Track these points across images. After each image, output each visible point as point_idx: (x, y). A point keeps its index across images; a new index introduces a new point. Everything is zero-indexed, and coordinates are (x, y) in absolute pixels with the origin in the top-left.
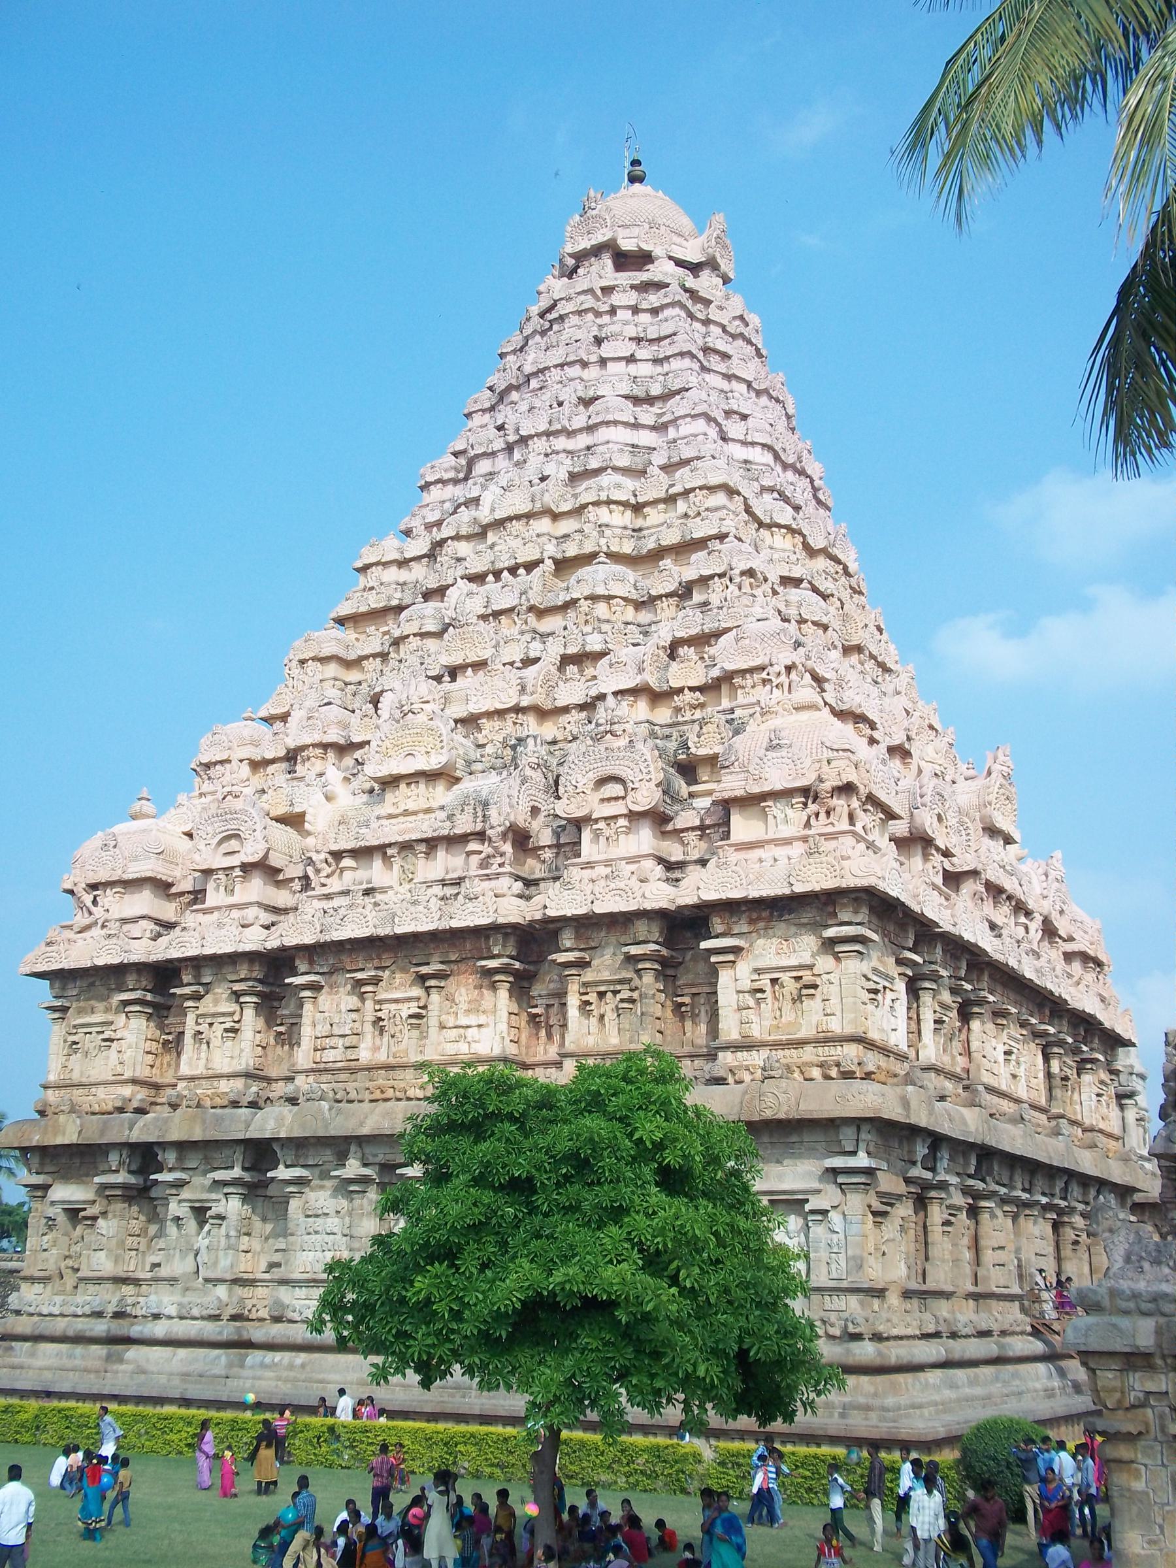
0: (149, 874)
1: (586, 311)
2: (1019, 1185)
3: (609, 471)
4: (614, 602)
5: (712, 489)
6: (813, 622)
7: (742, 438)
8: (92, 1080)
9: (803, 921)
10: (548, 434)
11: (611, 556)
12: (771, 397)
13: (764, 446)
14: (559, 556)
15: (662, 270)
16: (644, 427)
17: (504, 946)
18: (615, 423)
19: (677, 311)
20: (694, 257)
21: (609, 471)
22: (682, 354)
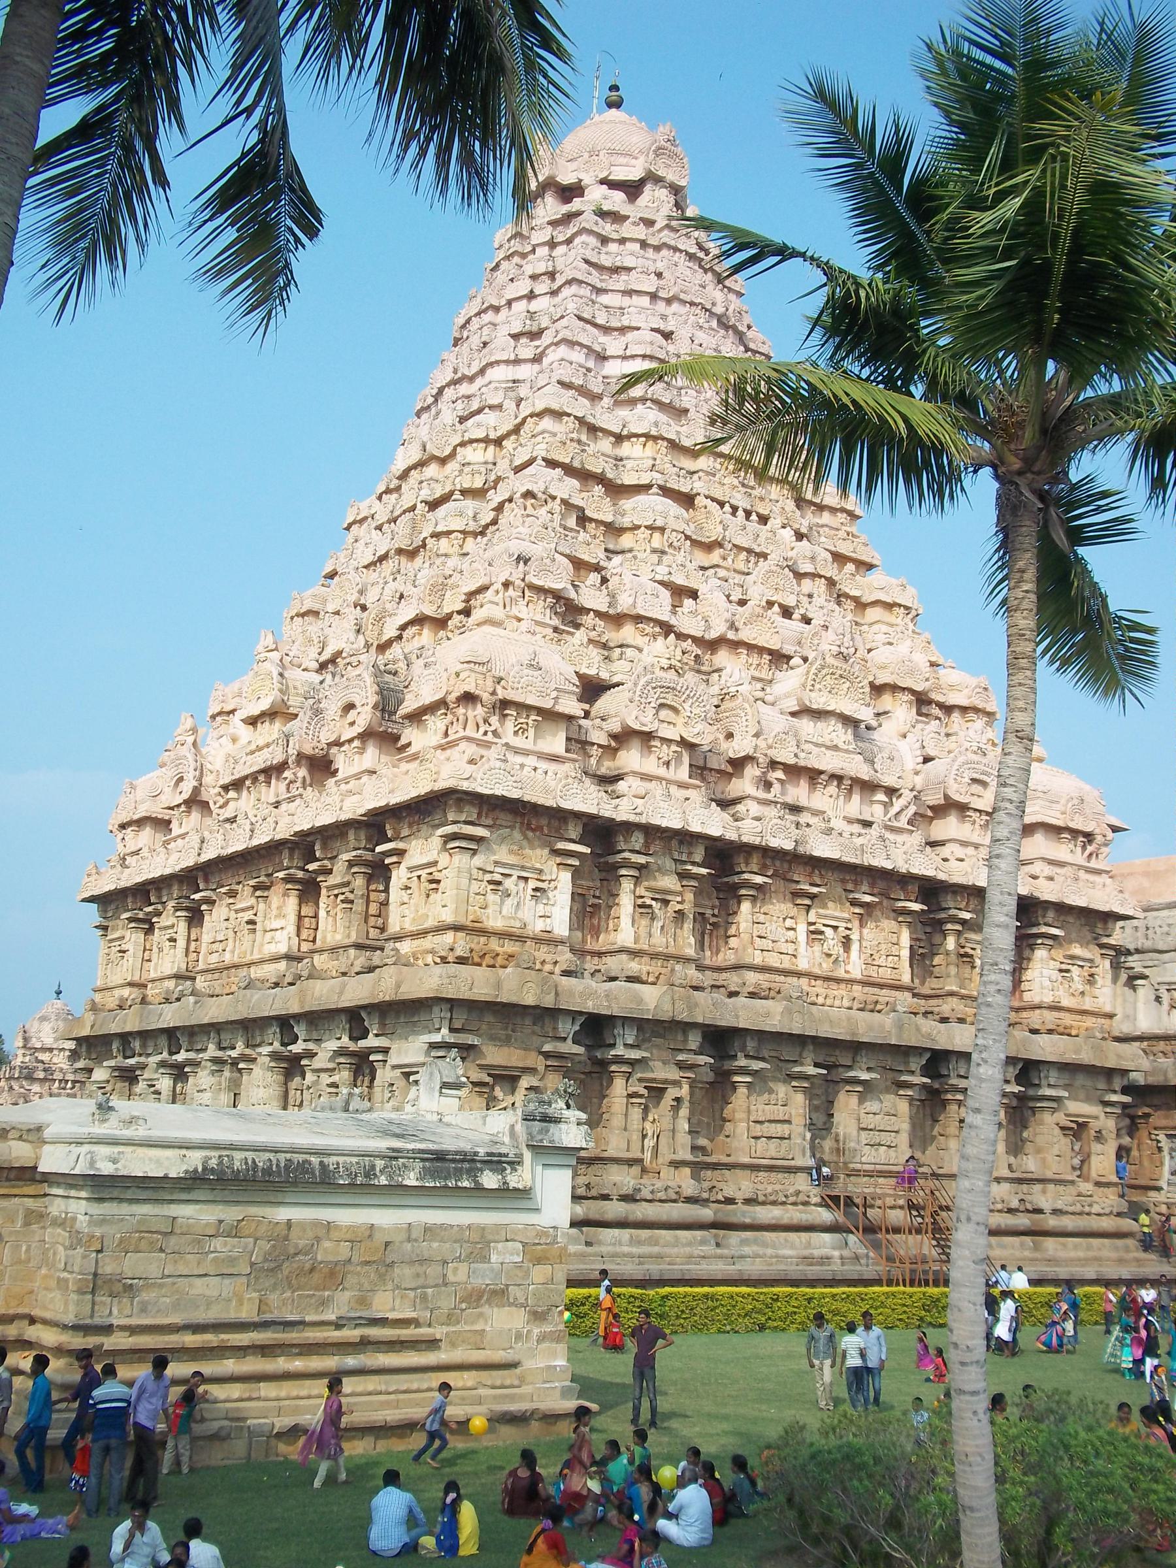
0: (148, 814)
1: (512, 255)
2: (809, 1060)
3: (487, 410)
4: (452, 536)
5: (539, 415)
6: (646, 527)
7: (621, 353)
8: (113, 985)
9: (437, 822)
10: (454, 382)
11: (464, 492)
12: (684, 302)
13: (644, 357)
14: (430, 499)
15: (596, 195)
16: (525, 361)
17: (291, 858)
18: (498, 362)
19: (584, 238)
20: (634, 173)
21: (487, 410)
22: (569, 282)
